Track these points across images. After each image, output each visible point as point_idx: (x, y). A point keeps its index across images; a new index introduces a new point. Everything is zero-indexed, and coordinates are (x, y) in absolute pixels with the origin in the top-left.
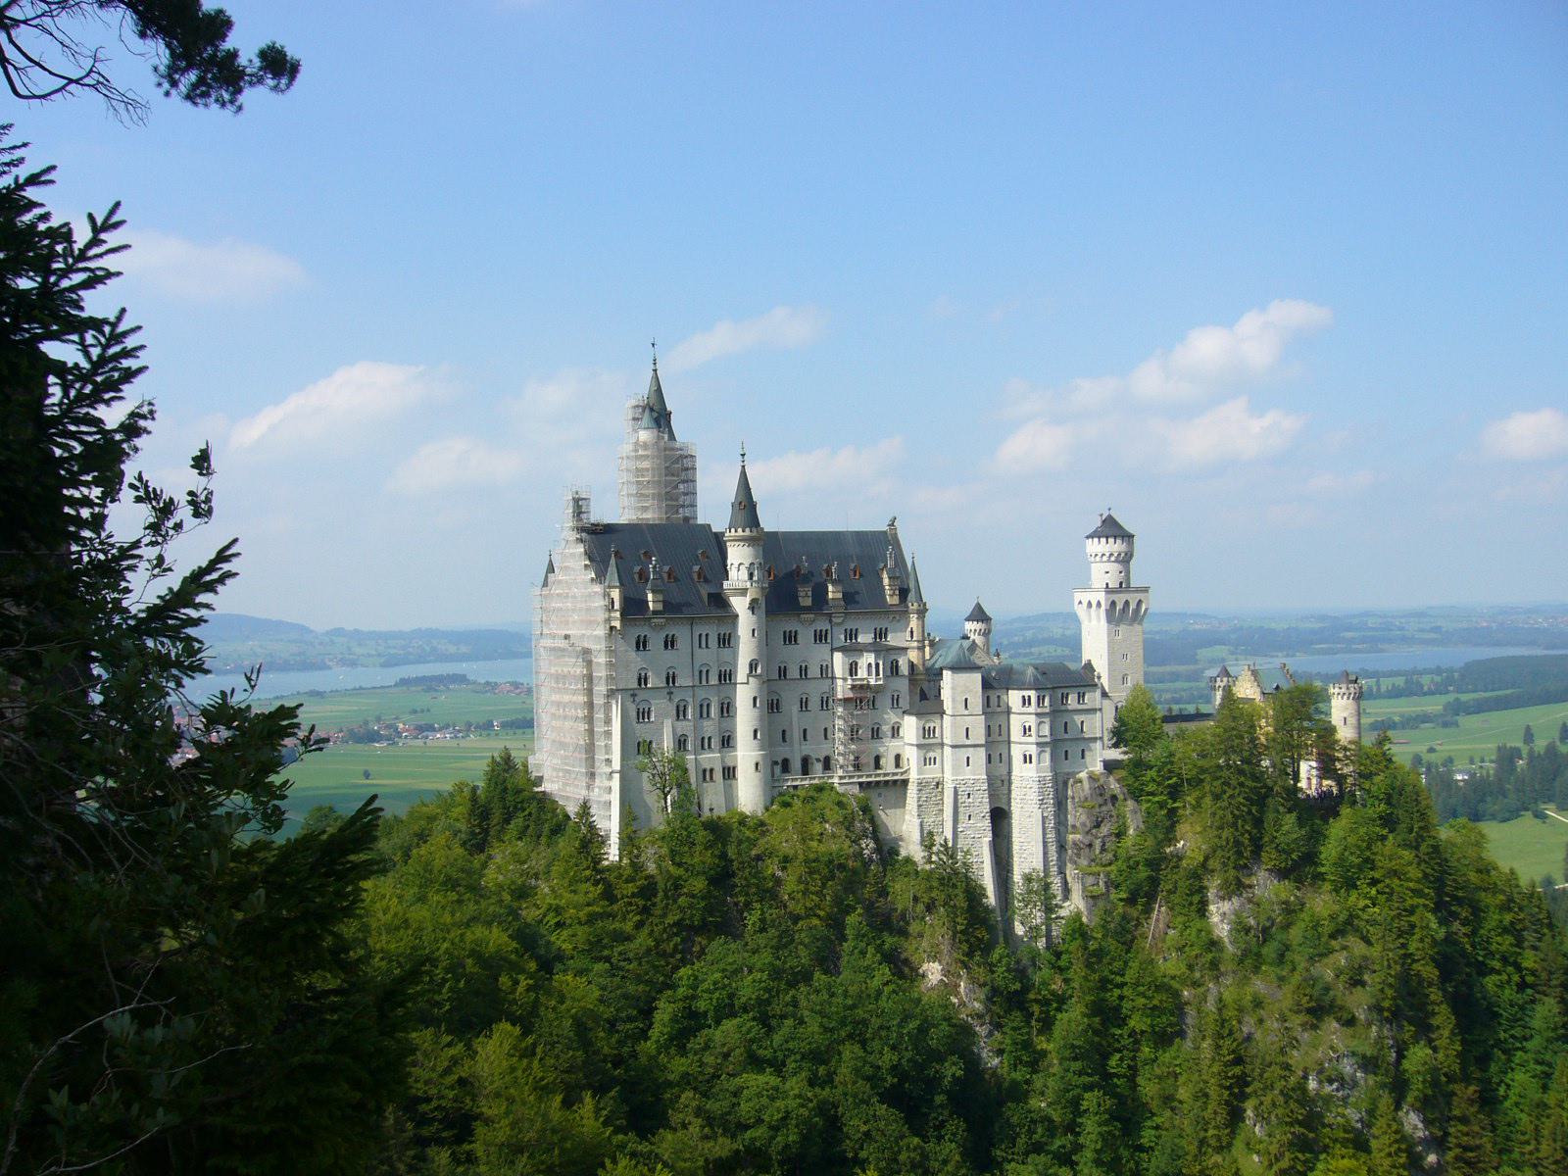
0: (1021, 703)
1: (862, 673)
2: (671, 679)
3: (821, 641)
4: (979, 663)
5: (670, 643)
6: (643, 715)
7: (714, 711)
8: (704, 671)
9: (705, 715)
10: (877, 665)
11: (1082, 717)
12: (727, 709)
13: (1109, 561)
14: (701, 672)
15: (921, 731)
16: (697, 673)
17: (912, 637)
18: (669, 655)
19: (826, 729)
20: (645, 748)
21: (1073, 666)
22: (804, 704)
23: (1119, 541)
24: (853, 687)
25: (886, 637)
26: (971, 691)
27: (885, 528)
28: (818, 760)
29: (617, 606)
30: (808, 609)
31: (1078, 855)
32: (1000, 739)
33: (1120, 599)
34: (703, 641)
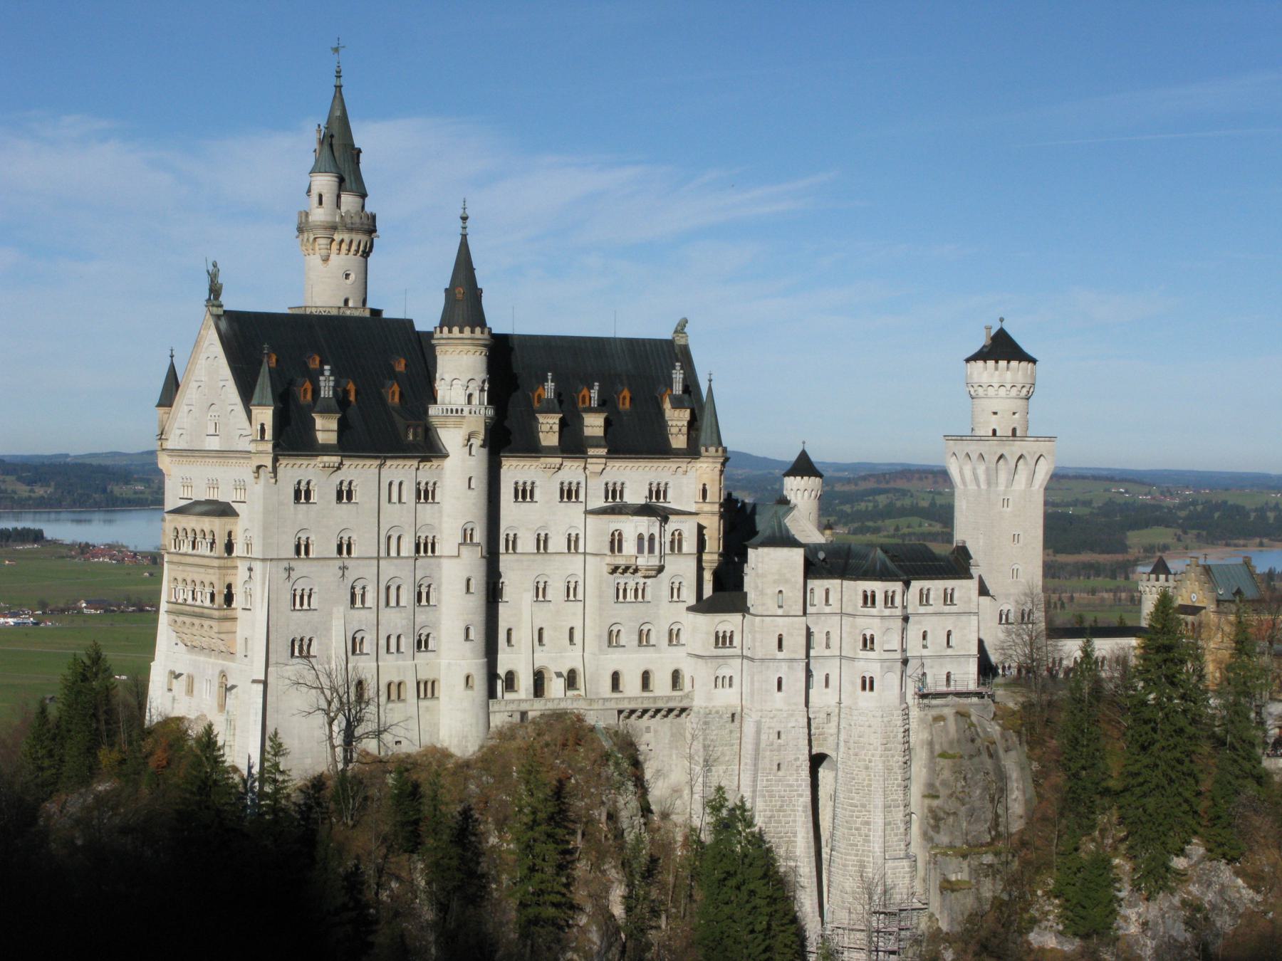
0: (861, 602)
1: (630, 547)
2: (344, 548)
3: (569, 497)
4: (802, 540)
6: (301, 599)
7: (407, 597)
9: (393, 602)
10: (652, 538)
11: (949, 623)
13: (997, 396)
14: (389, 538)
15: (713, 639)
16: (383, 540)
17: (704, 497)
19: (572, 629)
20: (301, 649)
21: (938, 549)
22: (540, 591)
23: (1014, 364)
24: (615, 570)
25: (665, 497)
26: (787, 581)
27: (667, 334)
28: (559, 675)
29: (269, 434)
31: (936, 828)
32: (827, 653)
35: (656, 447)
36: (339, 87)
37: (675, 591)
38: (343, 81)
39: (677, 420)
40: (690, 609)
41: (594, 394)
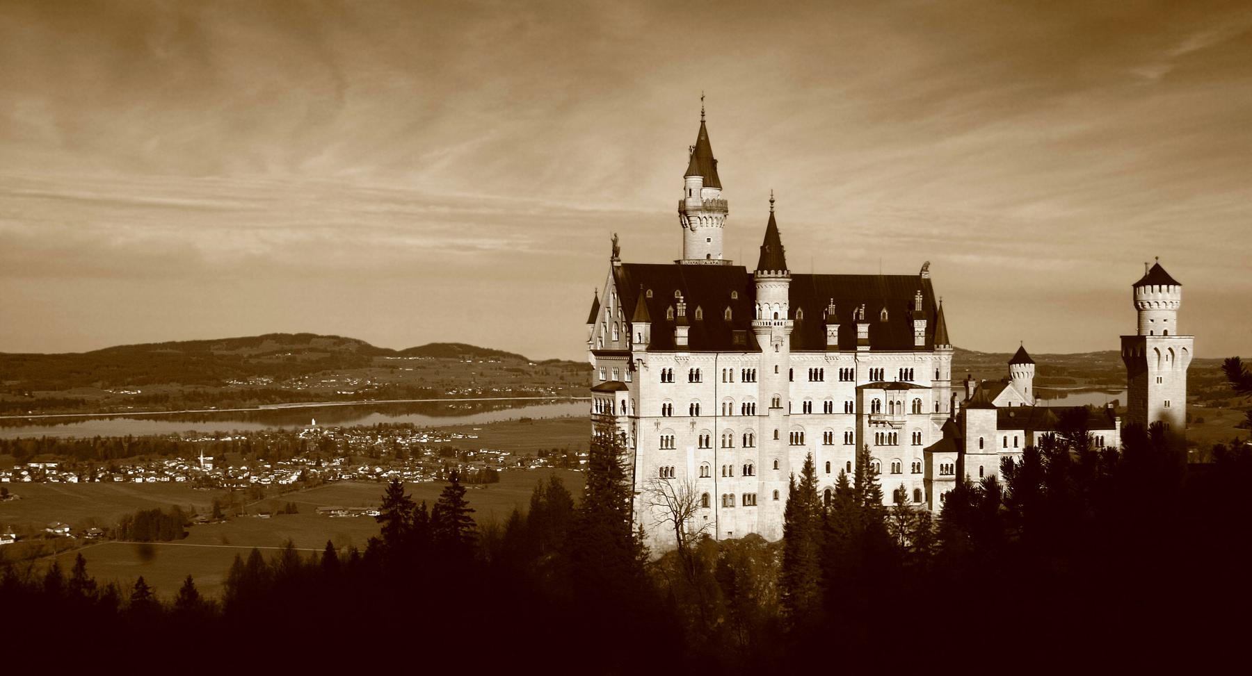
2: (695, 410)
5: (694, 376)
6: (667, 443)
7: (738, 441)
8: (728, 403)
9: (727, 445)
10: (899, 403)
12: (748, 441)
18: (693, 393)
20: (666, 473)
22: (828, 438)
23: (1164, 287)
26: (985, 431)
30: (833, 349)
33: (1164, 345)
34: (727, 376)
35: (906, 344)
36: (703, 122)
37: (917, 438)
38: (705, 118)
39: (920, 326)
40: (925, 450)
41: (862, 312)
